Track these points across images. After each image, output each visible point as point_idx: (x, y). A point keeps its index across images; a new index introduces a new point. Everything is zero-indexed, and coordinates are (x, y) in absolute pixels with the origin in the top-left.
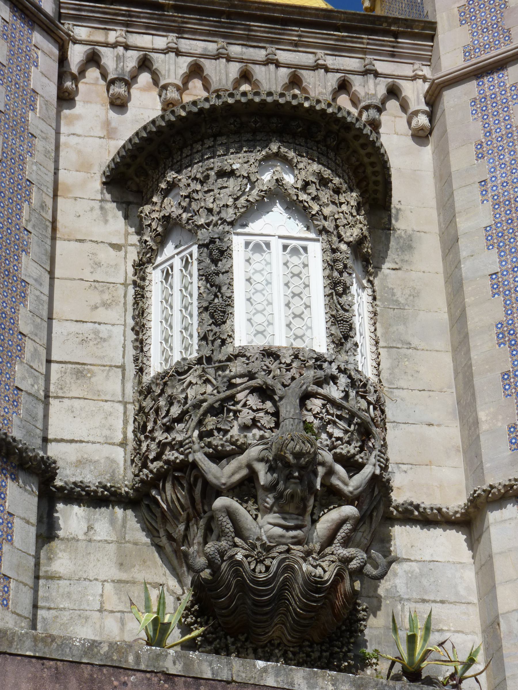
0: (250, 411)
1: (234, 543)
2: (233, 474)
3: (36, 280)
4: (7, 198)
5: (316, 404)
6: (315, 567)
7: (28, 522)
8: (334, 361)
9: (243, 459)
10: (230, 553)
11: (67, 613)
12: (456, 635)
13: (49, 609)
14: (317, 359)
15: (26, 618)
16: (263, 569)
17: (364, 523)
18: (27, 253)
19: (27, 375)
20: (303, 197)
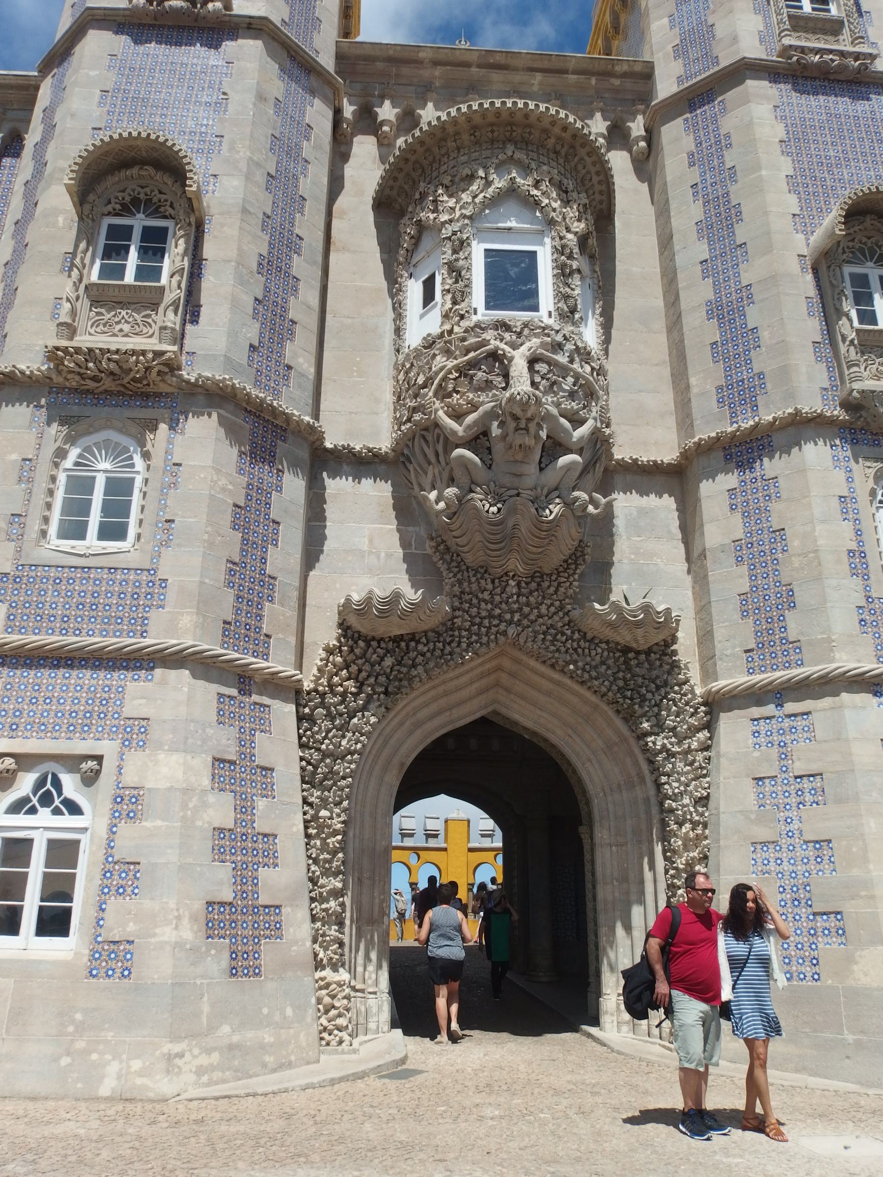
5: (542, 367)
14: (544, 329)
18: (299, 255)
20: (535, 192)
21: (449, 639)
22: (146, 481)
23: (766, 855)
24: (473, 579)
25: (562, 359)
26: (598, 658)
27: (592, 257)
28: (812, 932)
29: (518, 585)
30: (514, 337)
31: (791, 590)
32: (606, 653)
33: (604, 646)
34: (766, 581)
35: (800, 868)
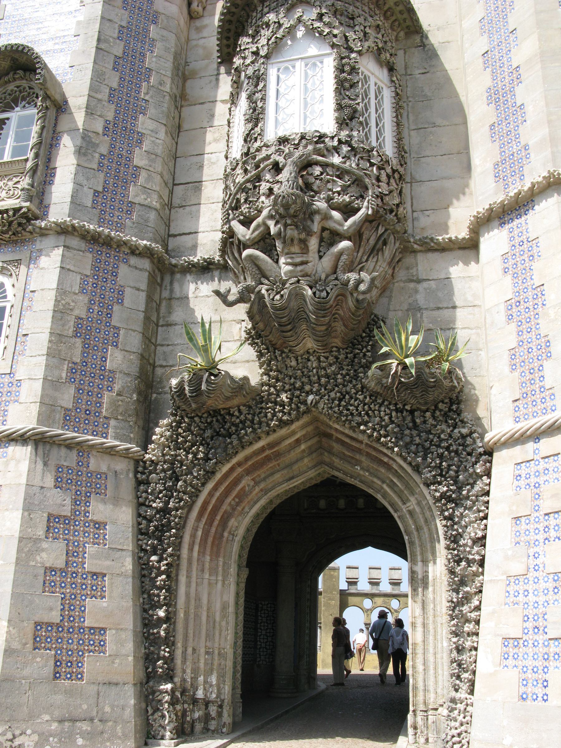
0: (268, 184)
1: (260, 281)
2: (254, 231)
3: (152, 131)
4: (127, 81)
5: (317, 170)
6: (322, 291)
7: (138, 289)
8: (335, 136)
9: (260, 219)
10: (257, 289)
11: (179, 347)
12: (463, 330)
13: (168, 345)
15: (134, 353)
16: (278, 297)
17: (377, 254)
19: (140, 193)
20: (317, 24)
21: (258, 411)
22: (12, 306)
23: (517, 588)
24: (280, 358)
25: (336, 160)
26: (386, 418)
27: (391, 69)
28: (546, 657)
29: (318, 358)
30: (292, 149)
31: (549, 341)
32: (394, 414)
33: (392, 407)
34: (529, 335)
35: (542, 599)
